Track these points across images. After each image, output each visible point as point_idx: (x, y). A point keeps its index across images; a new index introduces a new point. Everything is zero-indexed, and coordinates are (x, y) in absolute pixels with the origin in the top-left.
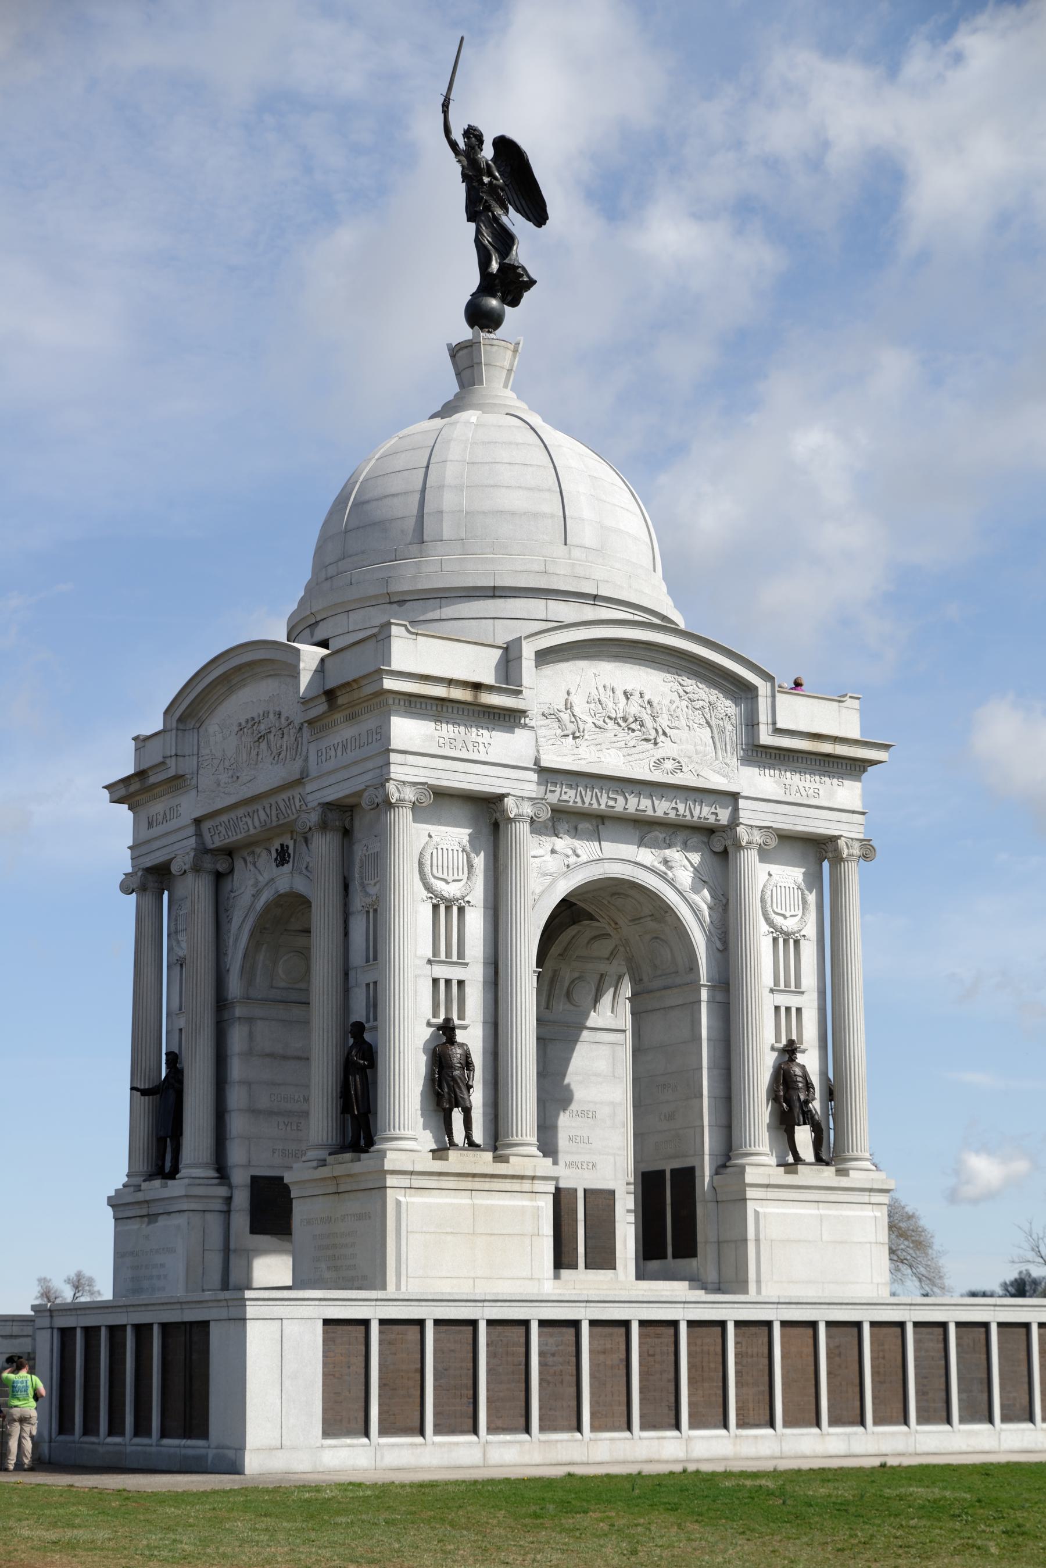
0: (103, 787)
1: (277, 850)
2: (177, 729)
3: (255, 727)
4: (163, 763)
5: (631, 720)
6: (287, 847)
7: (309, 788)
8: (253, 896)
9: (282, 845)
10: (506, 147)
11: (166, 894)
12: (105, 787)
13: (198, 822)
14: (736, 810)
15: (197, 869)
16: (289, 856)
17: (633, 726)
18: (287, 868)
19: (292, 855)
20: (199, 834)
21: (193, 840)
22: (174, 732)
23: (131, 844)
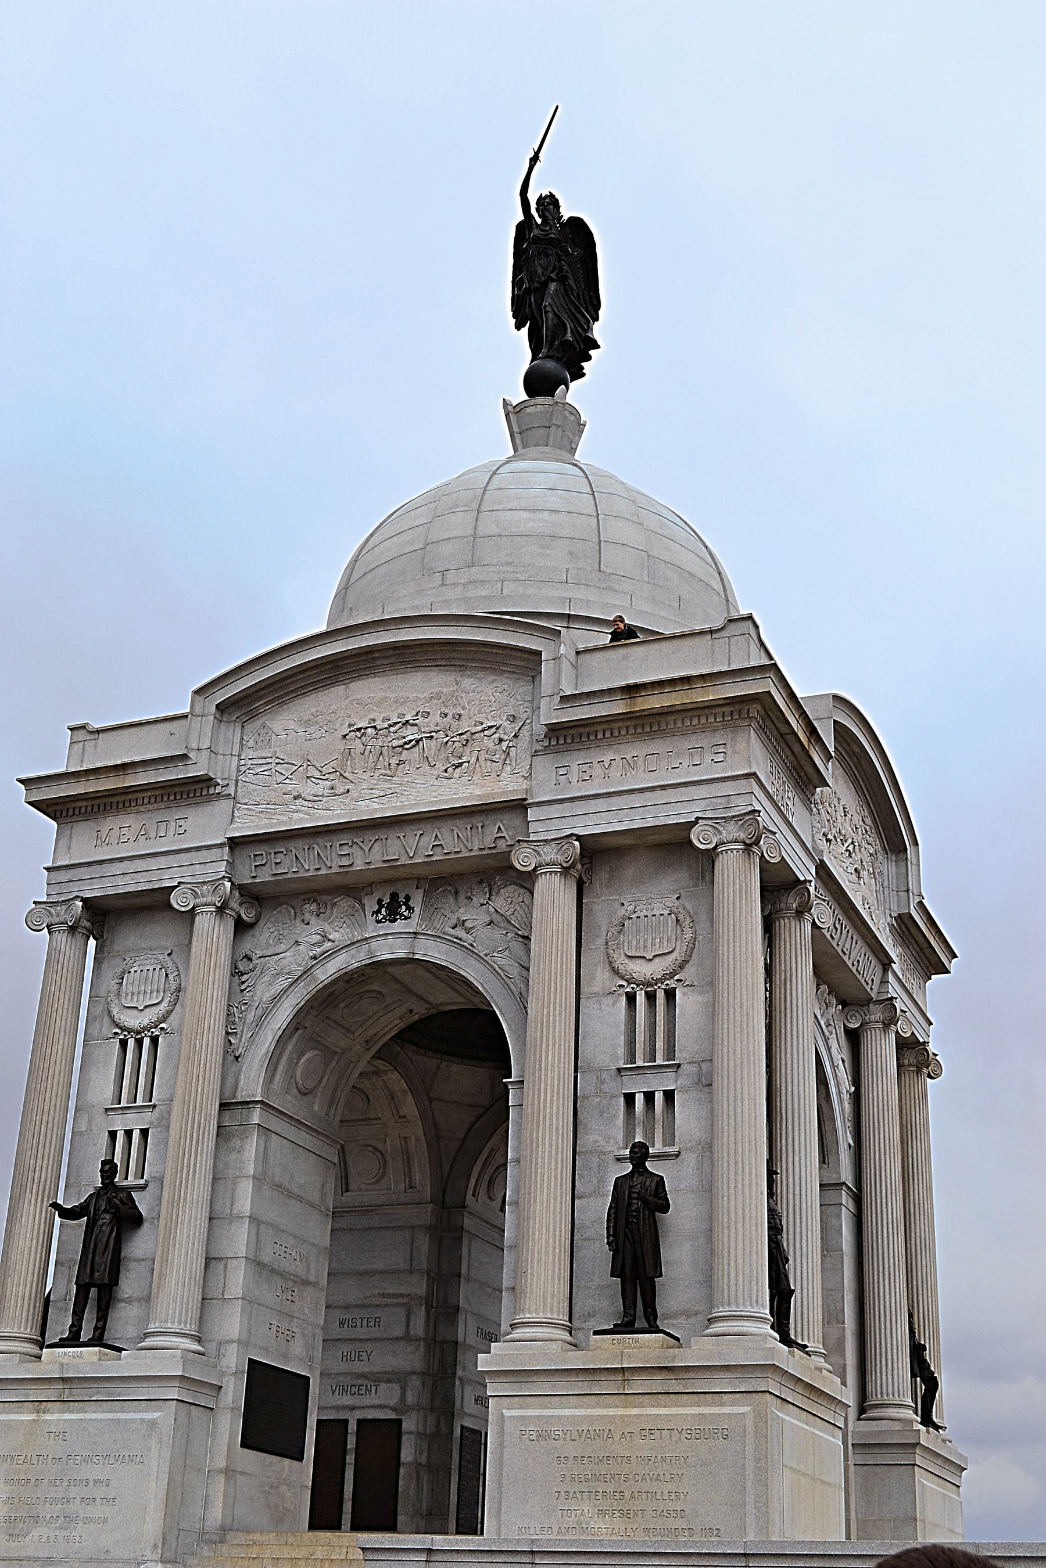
0: (21, 781)
1: (380, 902)
2: (215, 717)
3: (392, 729)
4: (184, 757)
5: (850, 841)
6: (408, 898)
7: (532, 814)
8: (315, 958)
9: (394, 896)
10: (578, 225)
11: (92, 942)
12: (21, 781)
13: (234, 844)
14: (884, 982)
15: (221, 910)
16: (409, 908)
17: (851, 848)
18: (399, 926)
19: (417, 910)
20: (231, 864)
21: (222, 867)
22: (212, 718)
23: (50, 864)
